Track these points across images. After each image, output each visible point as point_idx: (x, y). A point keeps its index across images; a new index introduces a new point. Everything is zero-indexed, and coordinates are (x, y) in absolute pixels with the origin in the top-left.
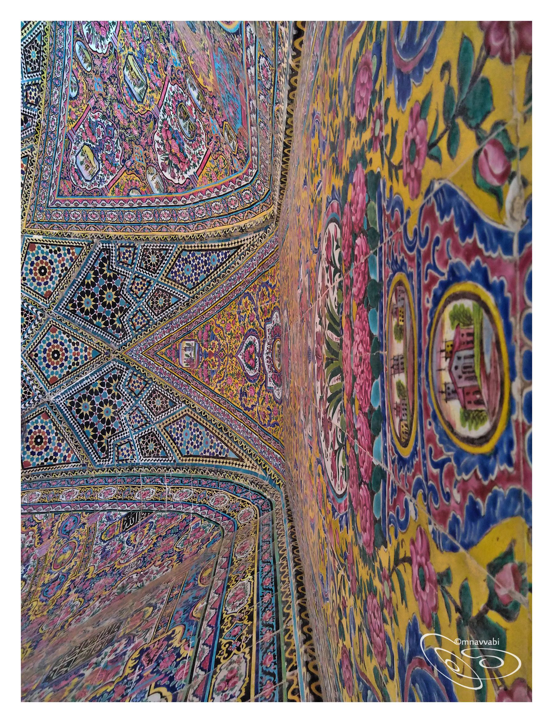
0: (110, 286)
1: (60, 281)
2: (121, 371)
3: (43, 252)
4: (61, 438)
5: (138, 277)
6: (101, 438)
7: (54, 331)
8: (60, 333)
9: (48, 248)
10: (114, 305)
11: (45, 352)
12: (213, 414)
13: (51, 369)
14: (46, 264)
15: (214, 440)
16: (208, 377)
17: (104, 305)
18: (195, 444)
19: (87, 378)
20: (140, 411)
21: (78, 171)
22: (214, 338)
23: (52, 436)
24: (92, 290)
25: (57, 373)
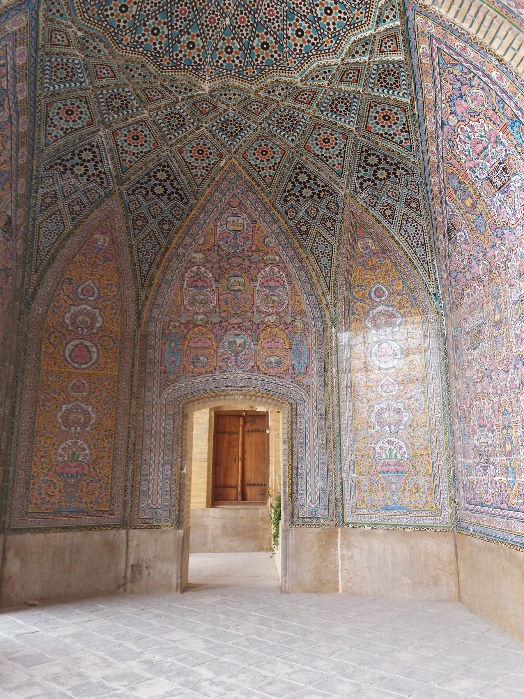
0: (165, 193)
1: (186, 162)
2: (105, 188)
3: (212, 159)
4: (67, 132)
5: (161, 212)
6: (61, 164)
7: (154, 144)
8: (150, 148)
9: (213, 164)
10: (152, 191)
11: (141, 131)
12: (63, 254)
13: (126, 133)
14: (204, 157)
15: (47, 249)
16: (84, 254)
17: (155, 185)
18: (47, 233)
19: (108, 164)
20: (73, 193)
21: (235, 215)
22: (105, 262)
23: (71, 124)
24: (169, 182)
25: (121, 137)
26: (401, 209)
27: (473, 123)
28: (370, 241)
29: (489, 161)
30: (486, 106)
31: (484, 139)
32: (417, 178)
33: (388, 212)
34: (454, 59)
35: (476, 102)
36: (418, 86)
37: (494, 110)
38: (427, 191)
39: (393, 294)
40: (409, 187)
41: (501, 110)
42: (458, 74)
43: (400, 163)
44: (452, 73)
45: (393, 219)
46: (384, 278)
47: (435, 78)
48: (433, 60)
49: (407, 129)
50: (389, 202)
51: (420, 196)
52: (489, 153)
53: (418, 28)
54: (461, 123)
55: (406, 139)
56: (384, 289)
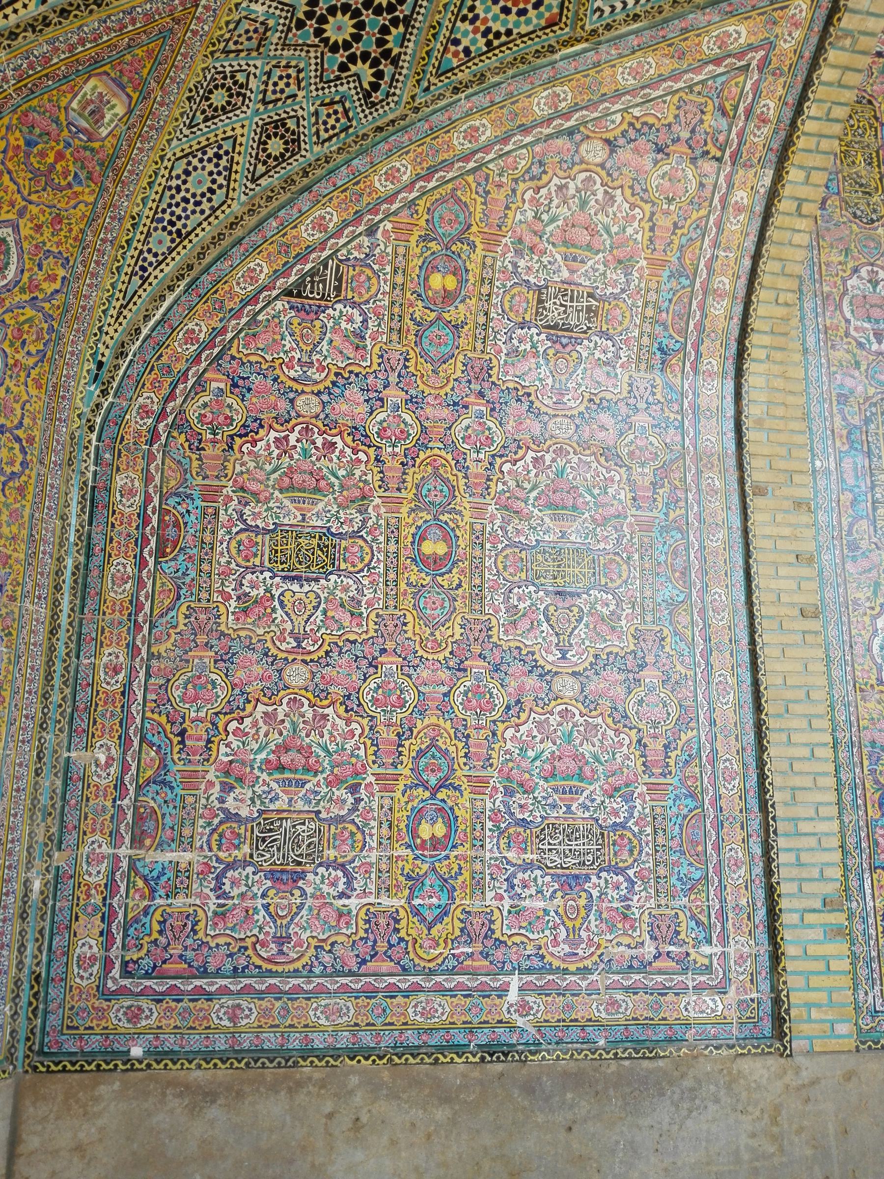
26: (245, 123)
27: (619, 199)
28: (120, 110)
29: (572, 271)
30: (672, 208)
31: (605, 236)
32: (364, 121)
33: (219, 98)
34: (736, 108)
35: (667, 184)
36: (633, 41)
37: (675, 225)
38: (347, 162)
39: (23, 291)
40: (324, 111)
41: (684, 240)
42: (706, 125)
43: (395, 62)
44: (703, 112)
45: (206, 120)
46: (38, 228)
47: (675, 77)
48: (717, 61)
49: (496, 43)
50: (253, 84)
51: (311, 151)
52: (590, 263)
53: (782, 8)
54: (603, 173)
55: (467, 51)
56: (14, 258)
